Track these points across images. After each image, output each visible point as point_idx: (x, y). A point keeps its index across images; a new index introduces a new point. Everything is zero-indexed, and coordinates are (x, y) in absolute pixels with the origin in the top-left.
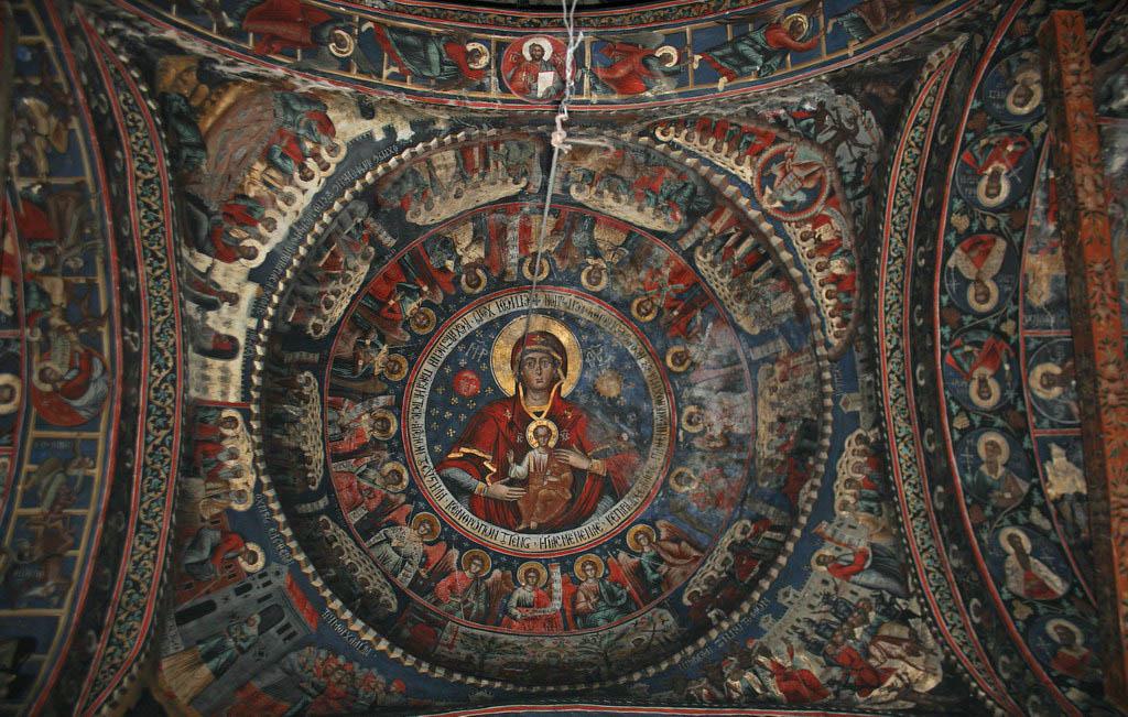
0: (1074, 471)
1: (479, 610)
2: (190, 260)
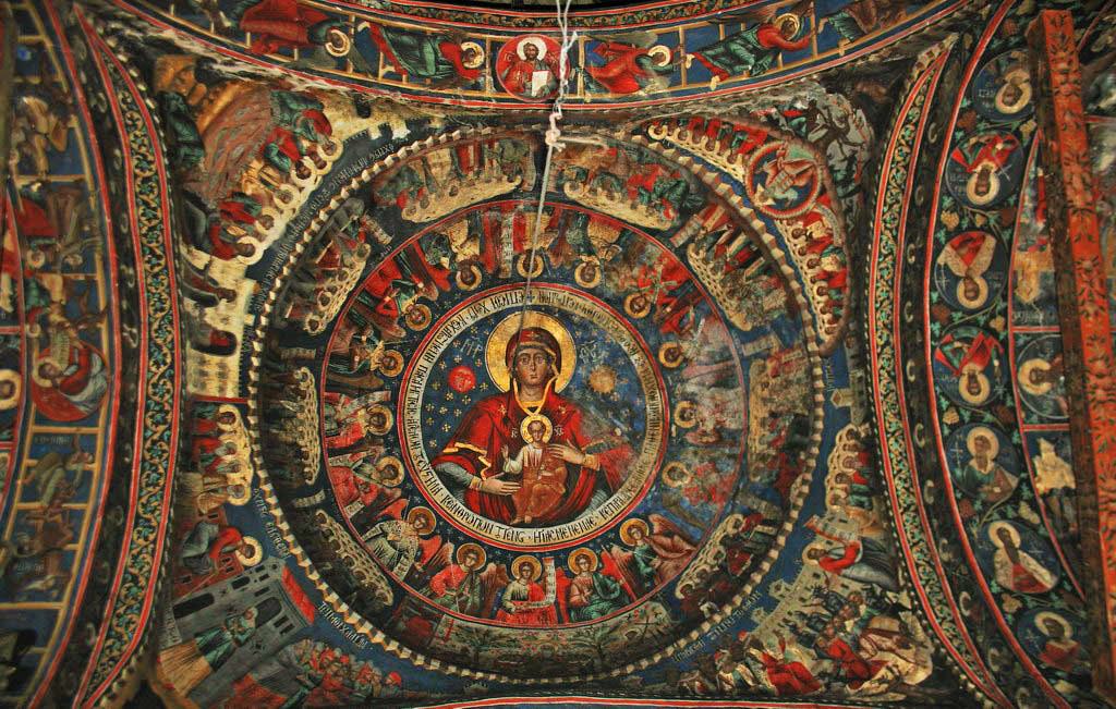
0: (1062, 466)
1: (474, 604)
2: (189, 258)
